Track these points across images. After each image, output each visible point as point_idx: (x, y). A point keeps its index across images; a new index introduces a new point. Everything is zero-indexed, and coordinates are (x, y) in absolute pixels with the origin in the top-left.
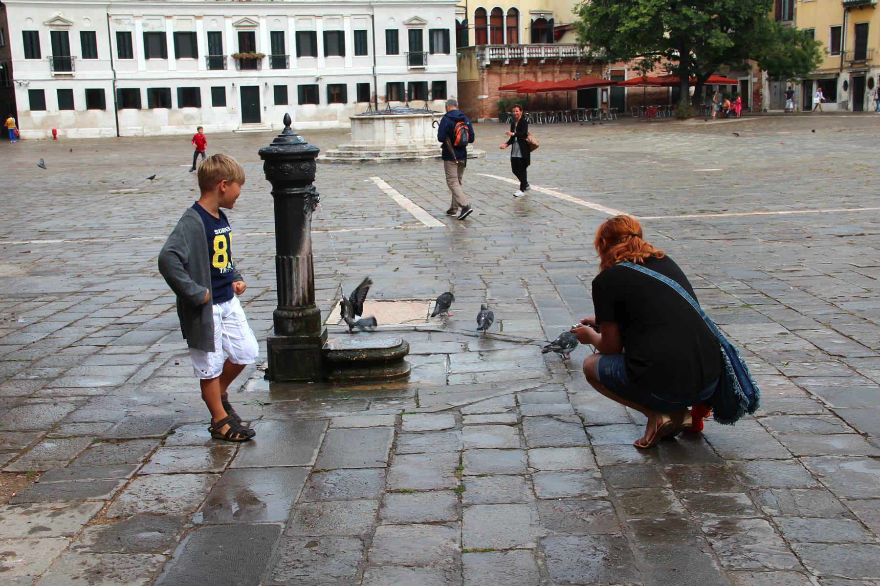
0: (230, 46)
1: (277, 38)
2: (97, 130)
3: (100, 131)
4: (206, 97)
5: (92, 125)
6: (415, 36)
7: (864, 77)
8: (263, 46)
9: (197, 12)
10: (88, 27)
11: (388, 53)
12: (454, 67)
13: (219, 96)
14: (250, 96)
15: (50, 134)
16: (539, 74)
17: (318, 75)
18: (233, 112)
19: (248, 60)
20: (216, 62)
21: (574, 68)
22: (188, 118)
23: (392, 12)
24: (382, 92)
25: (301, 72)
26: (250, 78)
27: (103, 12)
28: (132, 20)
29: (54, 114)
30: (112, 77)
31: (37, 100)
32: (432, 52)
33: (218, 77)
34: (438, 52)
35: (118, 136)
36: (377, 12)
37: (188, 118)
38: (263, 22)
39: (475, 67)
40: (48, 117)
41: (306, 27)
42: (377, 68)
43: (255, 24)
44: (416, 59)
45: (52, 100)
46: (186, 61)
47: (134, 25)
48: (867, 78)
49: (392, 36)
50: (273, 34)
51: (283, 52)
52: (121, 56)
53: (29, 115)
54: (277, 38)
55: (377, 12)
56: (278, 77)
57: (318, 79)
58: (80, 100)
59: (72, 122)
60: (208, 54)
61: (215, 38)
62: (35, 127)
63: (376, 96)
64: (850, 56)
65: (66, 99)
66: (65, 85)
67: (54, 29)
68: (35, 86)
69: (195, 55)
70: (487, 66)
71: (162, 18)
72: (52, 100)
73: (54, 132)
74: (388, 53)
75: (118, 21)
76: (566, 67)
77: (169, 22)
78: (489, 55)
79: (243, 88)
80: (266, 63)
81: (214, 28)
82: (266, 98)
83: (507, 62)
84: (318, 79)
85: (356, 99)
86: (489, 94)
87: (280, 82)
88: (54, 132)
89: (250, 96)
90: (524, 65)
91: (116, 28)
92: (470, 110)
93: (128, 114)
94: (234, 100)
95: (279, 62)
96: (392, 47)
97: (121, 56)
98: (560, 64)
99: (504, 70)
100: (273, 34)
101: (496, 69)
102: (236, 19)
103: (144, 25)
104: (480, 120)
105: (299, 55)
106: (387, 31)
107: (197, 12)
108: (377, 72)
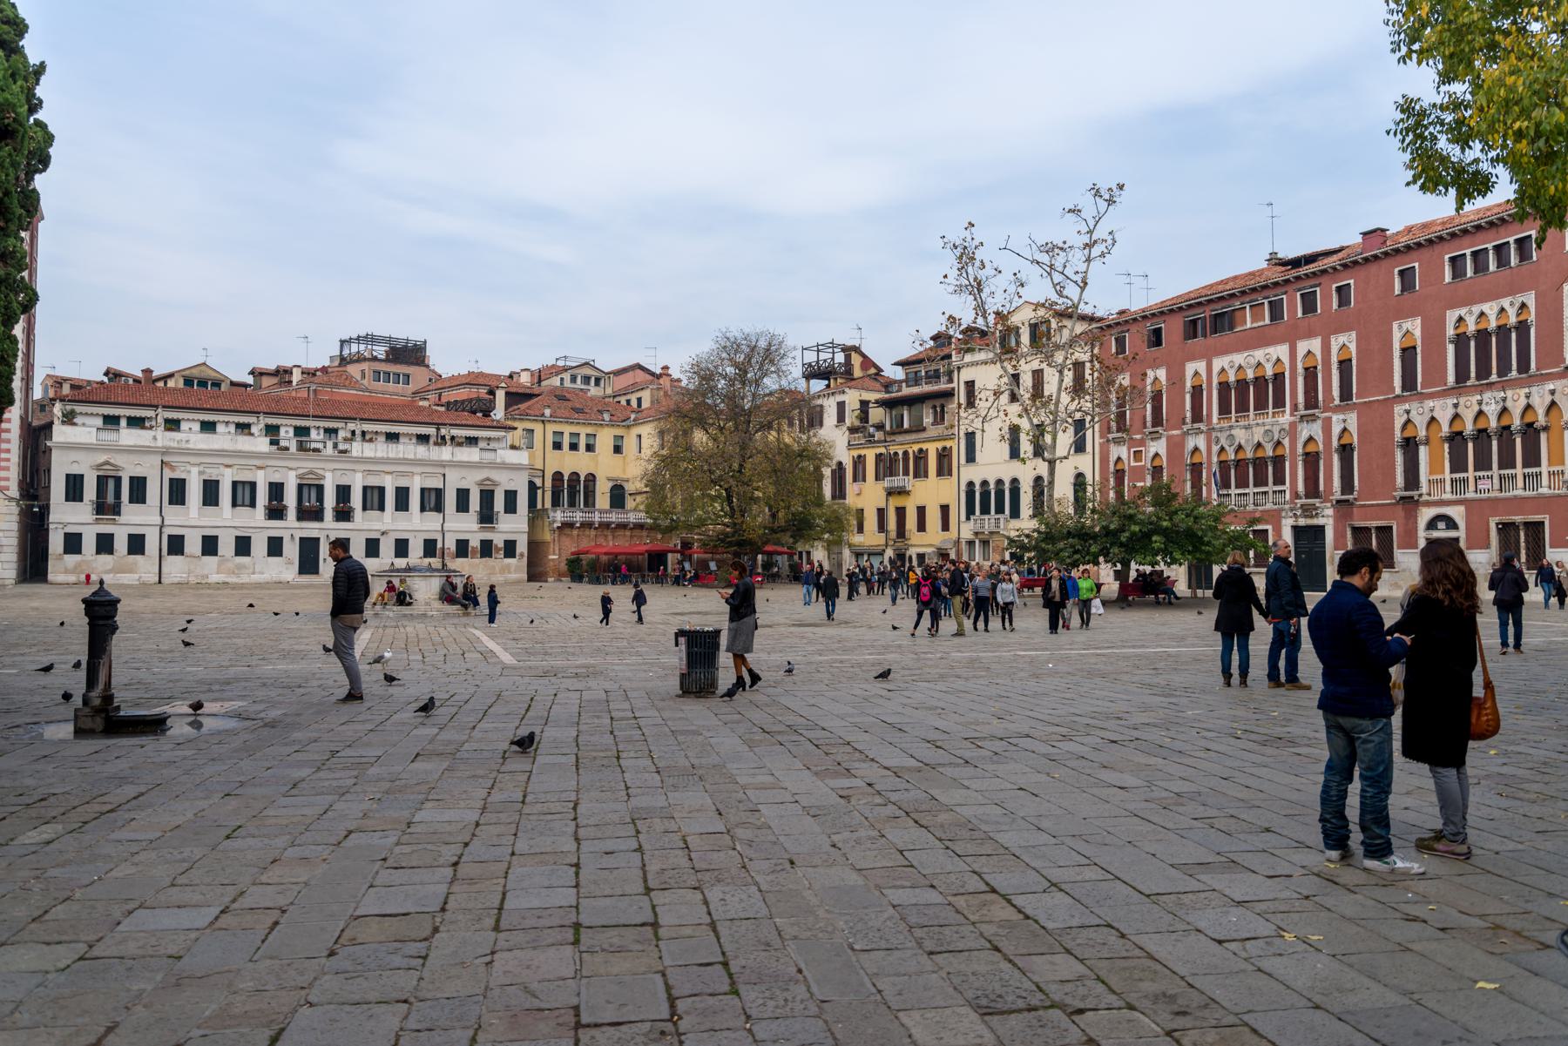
0: (290, 499)
1: (343, 492)
2: (136, 576)
3: (140, 577)
5: (131, 571)
6: (487, 497)
7: (904, 555)
9: (258, 462)
10: (138, 472)
11: (457, 511)
12: (525, 527)
13: (275, 547)
15: (83, 578)
16: (610, 537)
17: (384, 528)
18: (290, 562)
20: (276, 512)
21: (645, 533)
22: (240, 567)
23: (464, 472)
24: (451, 545)
26: (311, 529)
27: (156, 460)
28: (188, 467)
29: (91, 558)
30: (159, 522)
31: (73, 543)
33: (276, 528)
35: (160, 582)
36: (447, 471)
37: (240, 567)
38: (329, 475)
39: (547, 529)
40: (83, 561)
41: (373, 481)
42: (445, 525)
44: (487, 517)
45: (89, 544)
47: (189, 472)
48: (907, 556)
49: (463, 497)
53: (62, 559)
54: (343, 492)
55: (447, 471)
57: (383, 533)
58: (121, 544)
59: (109, 567)
61: (276, 490)
62: (66, 571)
63: (443, 553)
64: (893, 534)
66: (105, 529)
67: (101, 473)
69: (253, 504)
70: (558, 528)
71: (222, 468)
72: (89, 544)
73: (88, 577)
74: (457, 511)
75: (172, 468)
76: (637, 532)
77: (228, 472)
78: (559, 516)
79: (302, 539)
80: (329, 514)
81: (277, 478)
83: (578, 525)
84: (383, 533)
85: (422, 554)
86: (560, 555)
87: (342, 535)
88: (88, 577)
90: (596, 528)
91: (168, 474)
92: (541, 569)
94: (292, 550)
95: (343, 514)
96: (463, 505)
98: (631, 529)
99: (575, 532)
101: (567, 531)
102: (301, 471)
104: (550, 579)
105: (365, 508)
106: (458, 490)
107: (258, 462)
108: (445, 529)
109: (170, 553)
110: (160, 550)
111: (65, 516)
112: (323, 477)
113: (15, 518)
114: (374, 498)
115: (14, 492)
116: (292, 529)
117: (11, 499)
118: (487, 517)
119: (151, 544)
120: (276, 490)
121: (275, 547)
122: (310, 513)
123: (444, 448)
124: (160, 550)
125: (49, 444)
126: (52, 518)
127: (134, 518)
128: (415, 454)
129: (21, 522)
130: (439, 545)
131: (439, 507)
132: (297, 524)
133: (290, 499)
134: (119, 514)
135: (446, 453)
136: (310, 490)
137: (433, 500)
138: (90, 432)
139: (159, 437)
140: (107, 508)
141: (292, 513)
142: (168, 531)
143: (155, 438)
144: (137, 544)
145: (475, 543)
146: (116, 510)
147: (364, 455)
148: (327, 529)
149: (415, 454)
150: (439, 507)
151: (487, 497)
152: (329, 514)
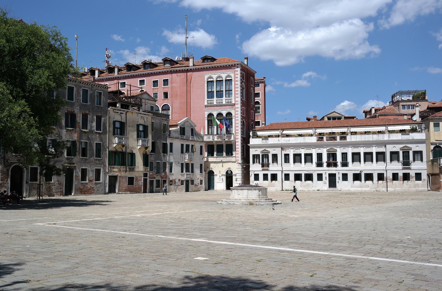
1: (344, 155)
2: (275, 188)
3: (276, 188)
4: (315, 177)
5: (273, 186)
6: (406, 154)
8: (339, 159)
10: (274, 152)
13: (320, 177)
14: (332, 177)
18: (325, 183)
19: (332, 163)
20: (320, 164)
24: (390, 176)
25: (354, 168)
26: (332, 170)
31: (257, 177)
32: (414, 160)
33: (320, 170)
34: (418, 161)
37: (308, 185)
43: (335, 150)
46: (308, 164)
47: (290, 151)
50: (343, 154)
51: (347, 161)
52: (285, 162)
54: (344, 155)
56: (344, 170)
60: (316, 161)
61: (320, 156)
65: (265, 177)
66: (266, 172)
68: (256, 173)
69: (312, 162)
82: (339, 177)
89: (332, 177)
93: (286, 183)
95: (345, 164)
97: (285, 162)
100: (343, 154)
103: (294, 151)
109: (285, 180)
110: (282, 179)
111: (255, 168)
112: (336, 151)
113: (240, 169)
114: (356, 157)
115: (240, 161)
116: (326, 171)
117: (240, 164)
118: (406, 163)
119: (279, 177)
120: (320, 156)
121: (320, 177)
122: (332, 163)
123: (385, 135)
124: (282, 179)
125: (248, 145)
126: (251, 169)
127: (273, 168)
128: (373, 138)
129: (242, 171)
130: (385, 176)
131: (384, 160)
132: (327, 168)
133: (325, 159)
134: (268, 167)
135: (386, 137)
136: (332, 156)
137: (381, 156)
138: (260, 140)
139: (280, 140)
140: (265, 165)
141: (325, 164)
142: (284, 172)
143: (279, 140)
144: (274, 177)
145: (401, 175)
146: (268, 165)
147: (352, 141)
148: (339, 170)
149: (373, 138)
150: (384, 160)
151: (406, 154)
152: (339, 164)
